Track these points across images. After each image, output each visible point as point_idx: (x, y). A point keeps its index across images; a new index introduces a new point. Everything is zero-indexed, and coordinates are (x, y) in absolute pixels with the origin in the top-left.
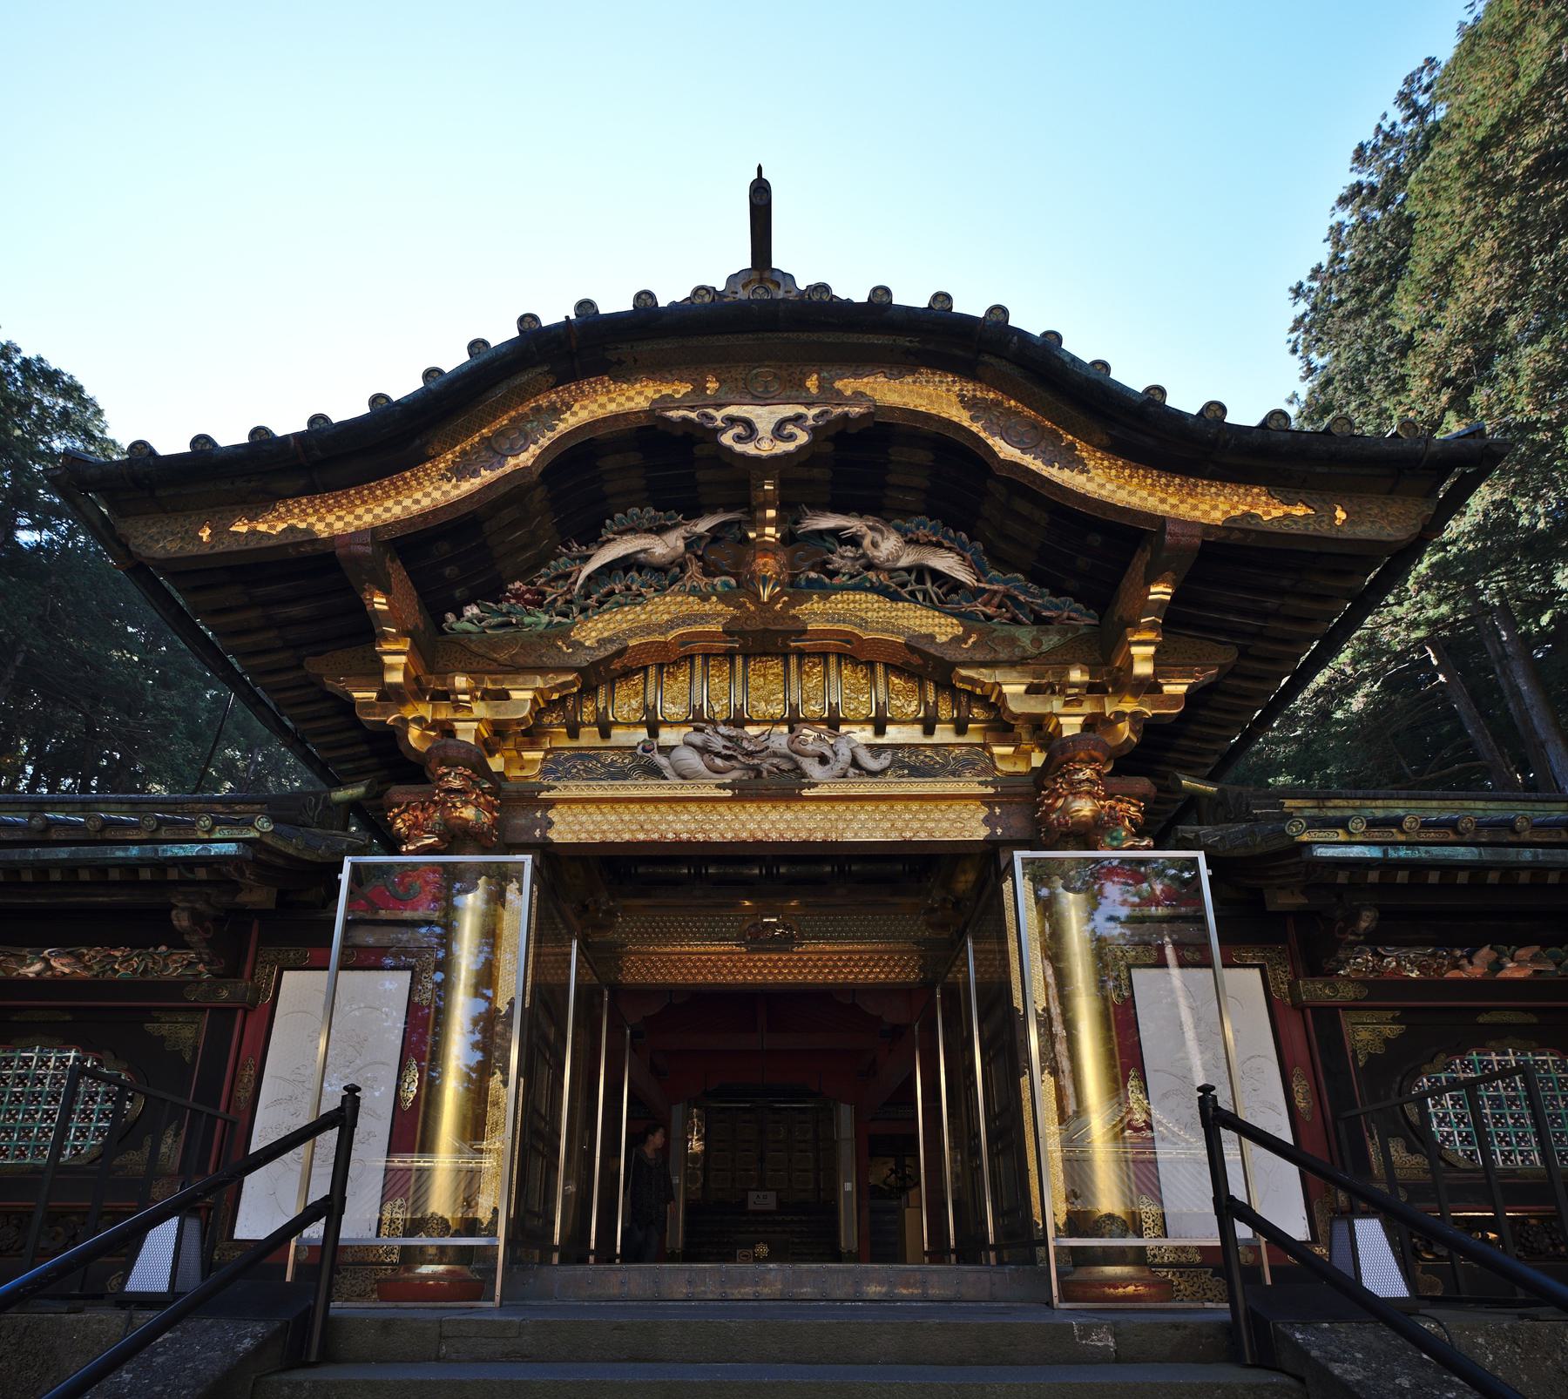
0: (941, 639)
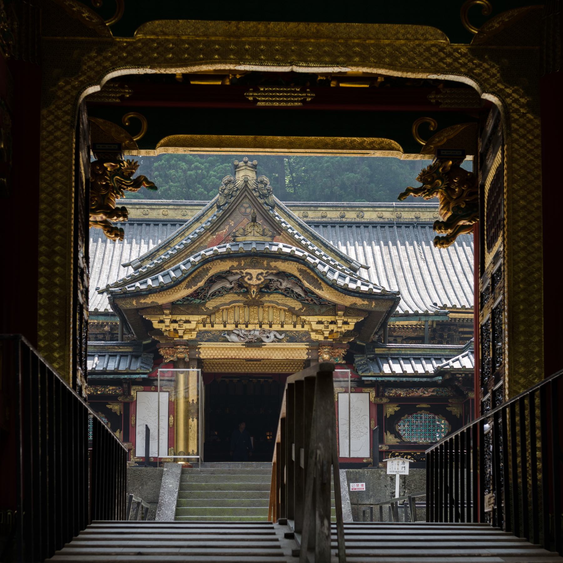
0: (297, 309)
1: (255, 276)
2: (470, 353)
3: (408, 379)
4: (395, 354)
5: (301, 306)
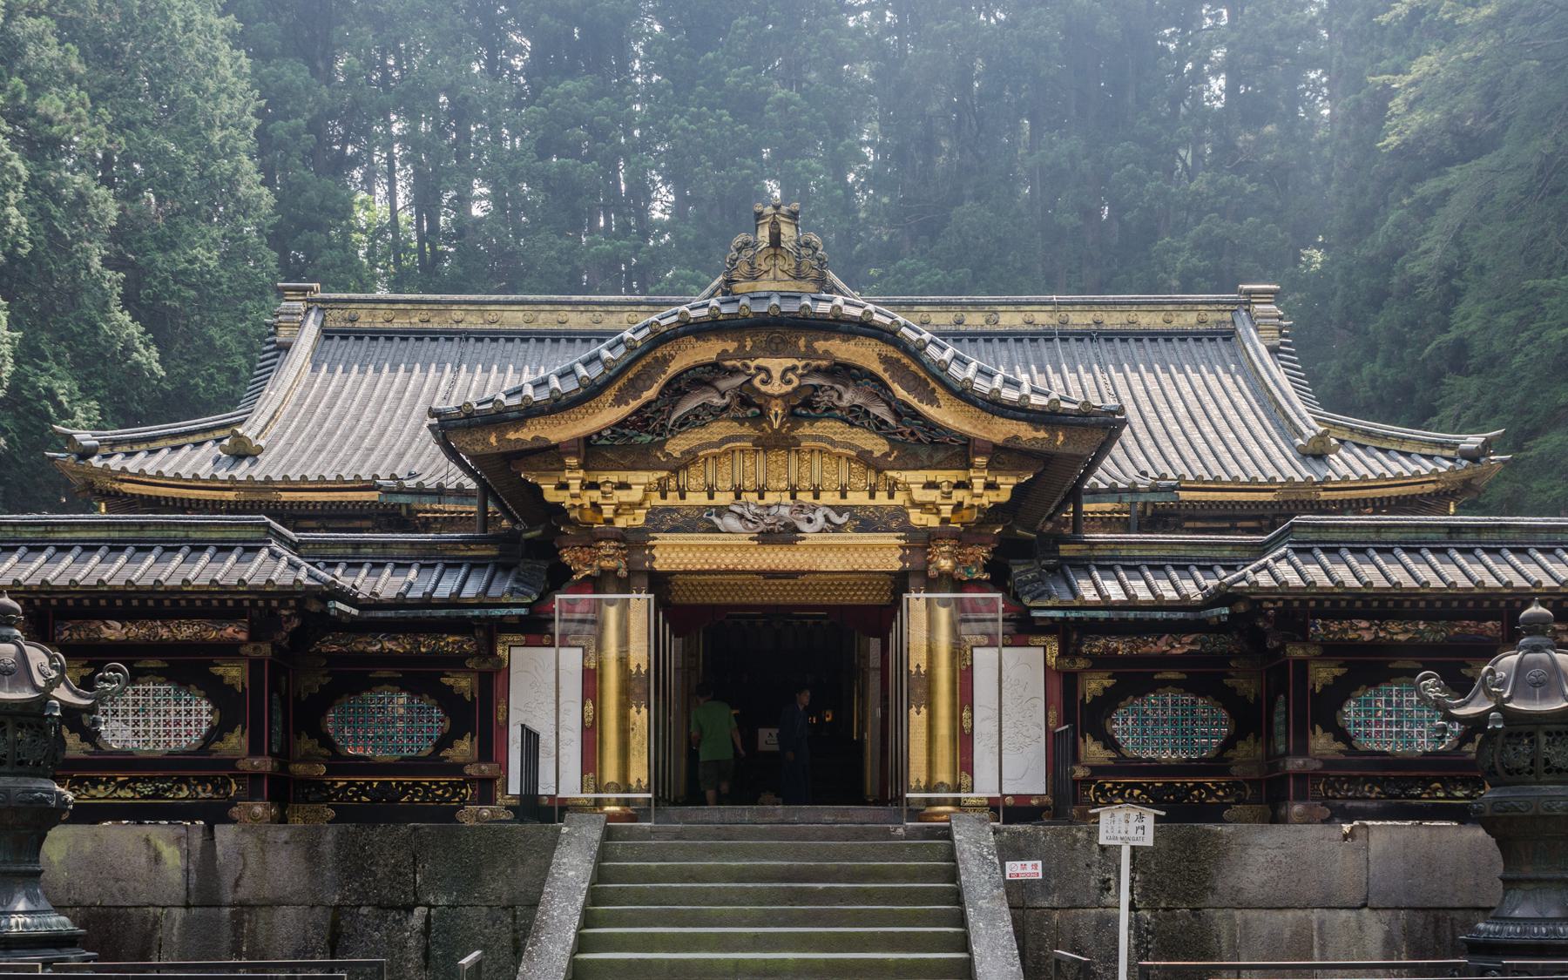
0: (877, 454)
1: (777, 373)
2: (1290, 553)
3: (1139, 614)
4: (1104, 558)
5: (887, 448)
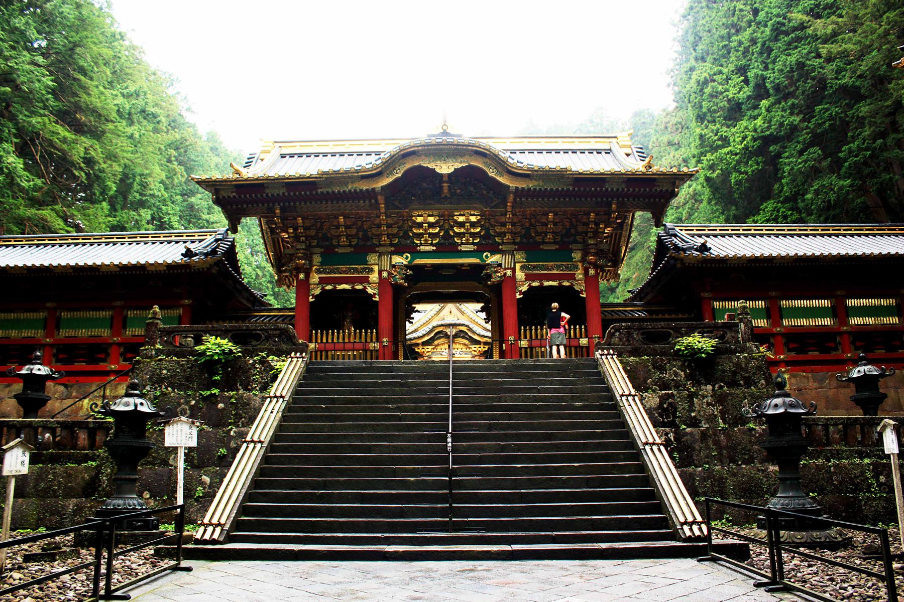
1: (451, 331)
